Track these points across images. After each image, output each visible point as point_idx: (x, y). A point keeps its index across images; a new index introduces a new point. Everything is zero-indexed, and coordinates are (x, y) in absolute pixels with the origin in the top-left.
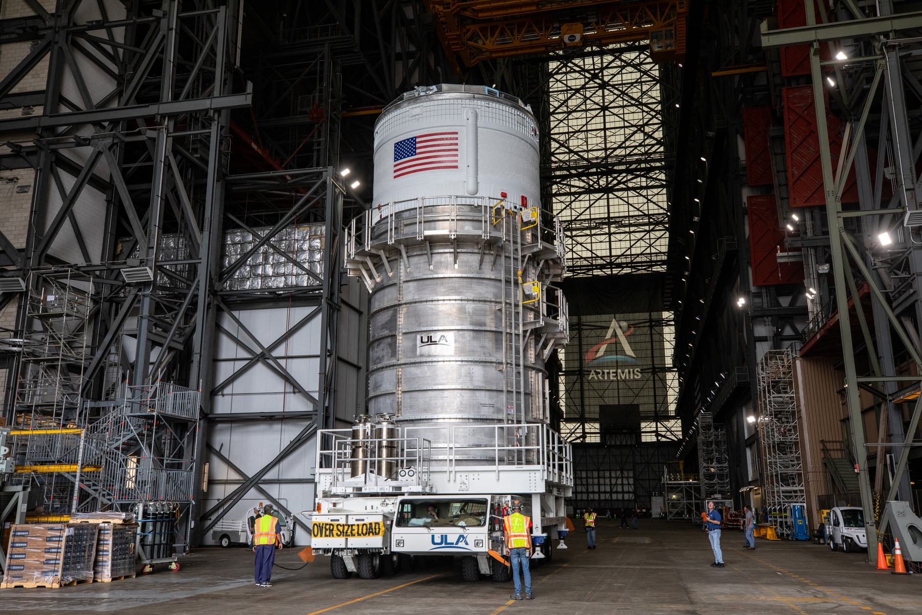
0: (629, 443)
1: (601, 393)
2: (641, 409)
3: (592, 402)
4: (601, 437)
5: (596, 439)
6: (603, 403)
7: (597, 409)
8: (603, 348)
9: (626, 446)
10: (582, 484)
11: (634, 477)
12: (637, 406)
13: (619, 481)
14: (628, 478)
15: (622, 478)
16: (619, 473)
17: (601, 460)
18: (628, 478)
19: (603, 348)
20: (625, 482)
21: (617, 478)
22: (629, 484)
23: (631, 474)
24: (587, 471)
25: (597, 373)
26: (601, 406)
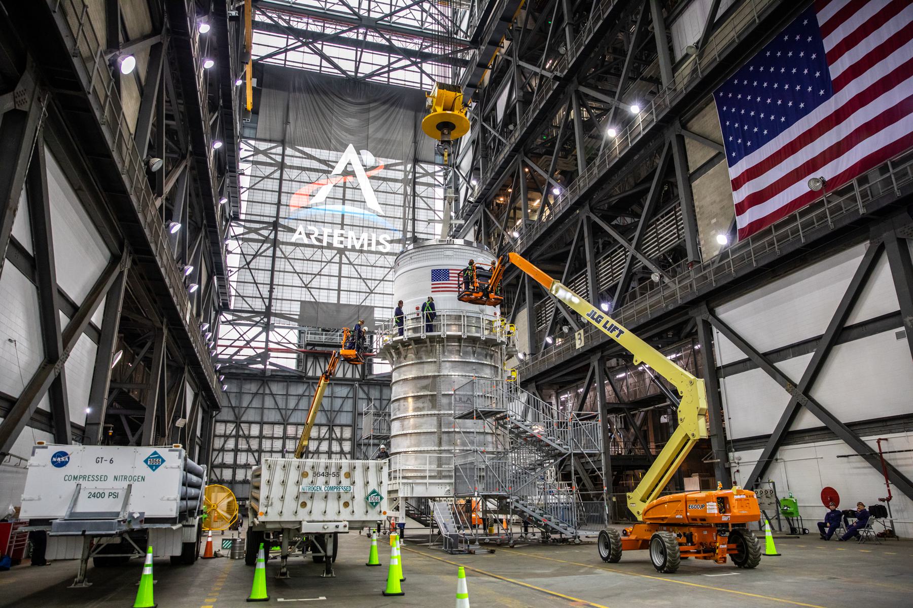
0: (349, 375)
1: (307, 279)
2: (378, 314)
3: (287, 293)
4: (299, 361)
5: (290, 363)
6: (308, 298)
7: (296, 308)
8: (325, 190)
9: (343, 382)
10: (249, 450)
11: (352, 439)
12: (371, 309)
13: (324, 447)
14: (341, 440)
15: (330, 439)
16: (324, 430)
17: (292, 405)
18: (341, 440)
19: (325, 190)
20: (336, 447)
21: (320, 440)
22: (342, 452)
23: (347, 433)
24: (262, 423)
25: (308, 235)
26: (303, 303)
